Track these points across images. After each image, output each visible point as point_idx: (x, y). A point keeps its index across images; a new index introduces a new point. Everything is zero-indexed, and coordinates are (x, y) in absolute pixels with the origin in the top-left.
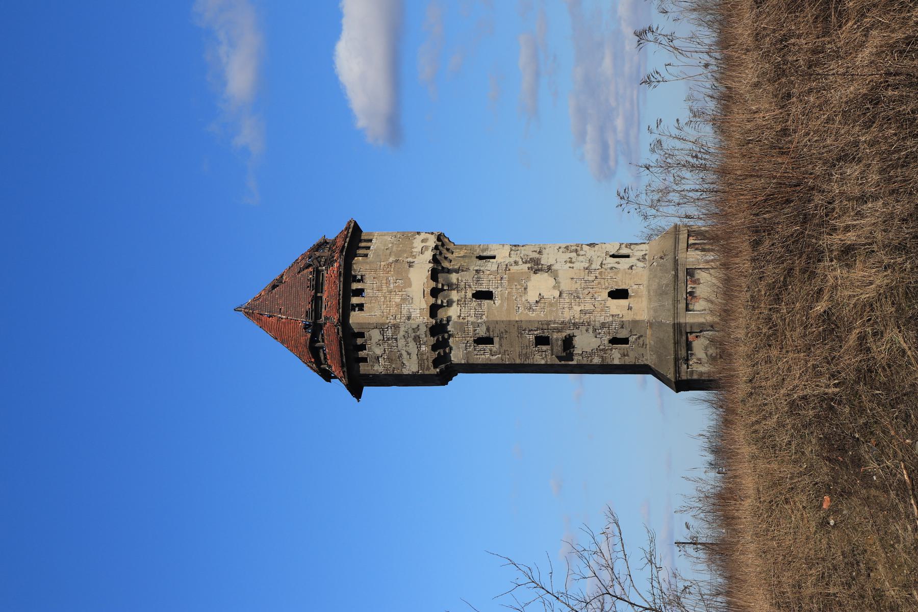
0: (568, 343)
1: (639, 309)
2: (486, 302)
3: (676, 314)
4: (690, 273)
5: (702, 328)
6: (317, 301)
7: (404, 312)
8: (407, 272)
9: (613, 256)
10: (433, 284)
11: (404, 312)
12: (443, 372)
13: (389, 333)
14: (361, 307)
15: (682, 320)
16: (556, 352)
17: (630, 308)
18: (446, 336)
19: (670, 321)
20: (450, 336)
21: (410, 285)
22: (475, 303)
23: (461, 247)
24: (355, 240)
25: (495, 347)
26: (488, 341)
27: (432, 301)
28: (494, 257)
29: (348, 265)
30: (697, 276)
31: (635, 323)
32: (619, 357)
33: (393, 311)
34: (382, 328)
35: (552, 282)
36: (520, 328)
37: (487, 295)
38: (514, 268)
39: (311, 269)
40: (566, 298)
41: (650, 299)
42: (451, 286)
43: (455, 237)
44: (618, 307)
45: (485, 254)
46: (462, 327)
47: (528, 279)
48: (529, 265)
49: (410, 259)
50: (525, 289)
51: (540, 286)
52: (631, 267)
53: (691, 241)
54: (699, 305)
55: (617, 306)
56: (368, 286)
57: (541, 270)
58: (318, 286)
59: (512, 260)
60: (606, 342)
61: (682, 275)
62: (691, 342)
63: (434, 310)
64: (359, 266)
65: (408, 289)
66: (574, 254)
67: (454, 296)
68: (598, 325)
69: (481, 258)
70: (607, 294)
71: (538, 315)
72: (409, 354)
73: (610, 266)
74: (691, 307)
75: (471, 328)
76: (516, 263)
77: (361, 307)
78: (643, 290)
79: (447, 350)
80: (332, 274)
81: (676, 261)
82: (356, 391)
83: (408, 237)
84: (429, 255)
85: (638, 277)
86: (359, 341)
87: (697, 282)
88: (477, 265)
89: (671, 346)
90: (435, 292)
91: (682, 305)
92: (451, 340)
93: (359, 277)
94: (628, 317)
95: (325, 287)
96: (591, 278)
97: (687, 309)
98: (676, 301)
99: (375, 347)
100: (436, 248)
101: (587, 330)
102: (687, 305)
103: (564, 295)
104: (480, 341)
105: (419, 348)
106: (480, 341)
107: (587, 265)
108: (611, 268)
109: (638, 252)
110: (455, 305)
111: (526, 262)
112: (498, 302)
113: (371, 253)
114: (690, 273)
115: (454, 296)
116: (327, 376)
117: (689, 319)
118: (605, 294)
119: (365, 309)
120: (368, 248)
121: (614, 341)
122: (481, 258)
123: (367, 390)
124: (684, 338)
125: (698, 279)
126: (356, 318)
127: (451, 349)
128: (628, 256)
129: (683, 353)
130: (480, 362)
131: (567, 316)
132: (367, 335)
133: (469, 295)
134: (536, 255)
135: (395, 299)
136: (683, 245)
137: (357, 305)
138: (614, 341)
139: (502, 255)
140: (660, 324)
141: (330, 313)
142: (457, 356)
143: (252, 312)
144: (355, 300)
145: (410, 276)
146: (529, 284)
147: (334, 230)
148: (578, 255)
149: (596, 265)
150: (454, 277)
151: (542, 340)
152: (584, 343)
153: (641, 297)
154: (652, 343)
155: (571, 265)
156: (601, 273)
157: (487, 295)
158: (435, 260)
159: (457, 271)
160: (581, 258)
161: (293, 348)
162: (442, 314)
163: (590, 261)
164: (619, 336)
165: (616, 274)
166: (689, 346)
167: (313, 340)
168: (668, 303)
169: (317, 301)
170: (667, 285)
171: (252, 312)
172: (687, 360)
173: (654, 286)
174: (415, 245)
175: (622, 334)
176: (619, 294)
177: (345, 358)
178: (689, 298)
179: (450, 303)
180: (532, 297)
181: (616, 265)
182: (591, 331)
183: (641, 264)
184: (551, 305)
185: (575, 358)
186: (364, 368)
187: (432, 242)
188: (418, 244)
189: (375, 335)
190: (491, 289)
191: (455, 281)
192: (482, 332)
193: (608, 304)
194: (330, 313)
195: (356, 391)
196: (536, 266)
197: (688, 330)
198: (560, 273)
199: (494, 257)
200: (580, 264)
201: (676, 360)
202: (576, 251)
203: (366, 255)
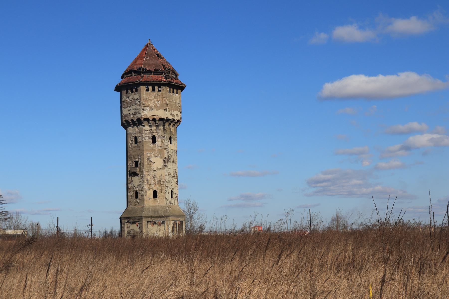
0: (135, 174)
1: (149, 202)
2: (151, 141)
3: (146, 217)
4: (163, 222)
5: (141, 228)
6: (150, 72)
7: (146, 108)
8: (162, 109)
9: (172, 191)
10: (157, 119)
11: (146, 108)
12: (126, 124)
13: (137, 102)
14: (148, 90)
15: (143, 220)
16: (134, 170)
17: (149, 199)
18: (137, 125)
19: (143, 215)
20: (138, 127)
21: (157, 110)
22: (151, 136)
23: (176, 130)
24: (180, 88)
25: (134, 145)
26: (136, 142)
27: (151, 119)
28: (171, 143)
29: (165, 84)
30: (162, 225)
31: (143, 201)
32: (134, 195)
33: (146, 103)
34: (139, 99)
35: (160, 167)
36: (141, 155)
37: (154, 141)
38: (165, 152)
39: (163, 69)
40: (153, 173)
41: (153, 206)
42: (157, 126)
43: (180, 128)
45: (172, 140)
46: (141, 131)
47: (161, 158)
48: (167, 157)
49: (168, 110)
51: (158, 162)
52: (166, 199)
53: (178, 222)
54: (150, 226)
55: (150, 193)
56: (156, 93)
57: (165, 162)
58: (157, 72)
59: (169, 151)
60: (136, 189)
61: (162, 219)
63: (147, 120)
64: (165, 89)
65: (155, 109)
66: (172, 175)
67: (154, 128)
68: (142, 186)
69: (170, 138)
71: (146, 162)
72: (130, 110)
73: (167, 190)
74: (149, 223)
75: (141, 135)
76: (168, 152)
77: (148, 90)
78: (157, 204)
79: (132, 126)
80: (162, 78)
81: (168, 216)
82: (118, 88)
83: (179, 108)
84: (170, 117)
85: (163, 201)
86: (134, 90)
87: (160, 225)
88: (167, 136)
89: (134, 216)
90: (154, 120)
91: (150, 220)
92: (136, 127)
93: (160, 89)
94: (146, 198)
95: (156, 76)
96: (161, 183)
97: (148, 222)
98: (151, 217)
99: (133, 96)
100: (174, 120)
103: (154, 172)
104: (136, 138)
105: (132, 114)
106: (136, 138)
107: (167, 181)
108: (166, 191)
109: (174, 201)
110: (150, 128)
111: (168, 156)
112: (151, 146)
113: (171, 94)
114: (163, 222)
115: (154, 128)
116: (122, 77)
117: (144, 222)
119: (147, 92)
120: (173, 92)
121: (137, 193)
122: (170, 138)
123: (119, 93)
124: (137, 221)
126: (143, 88)
127: (133, 127)
128: (172, 197)
129: (131, 220)
131: (146, 173)
134: (172, 160)
135: (152, 104)
136: (175, 219)
137: (148, 89)
138: (137, 193)
139: (172, 147)
140: (142, 211)
141: (144, 78)
142: (130, 129)
143: (149, 46)
144: (150, 88)
145: (161, 110)
146: (159, 158)
147: (182, 79)
148: (172, 177)
149: (167, 184)
150: (161, 128)
151: (136, 163)
152: (136, 181)
153: (154, 203)
155: (167, 175)
156: (164, 186)
157: (154, 141)
158: (168, 120)
159: (164, 129)
160: (171, 178)
161: (133, 64)
162: (146, 123)
163: (169, 182)
164: (138, 194)
165: (163, 193)
166: (134, 223)
167: (135, 72)
168: (151, 214)
169: (150, 72)
170: (158, 213)
171: (149, 46)
172: (128, 222)
173: (158, 208)
174: (175, 111)
175: (139, 196)
176: (155, 194)
177: (129, 85)
179: (150, 126)
180: (154, 159)
181: (167, 192)
182: (140, 183)
183: (168, 202)
184: (150, 167)
185: (130, 177)
186: (124, 92)
187: (176, 118)
188: (175, 113)
189: (136, 97)
191: (160, 128)
192: (139, 139)
194: (144, 78)
195: (118, 88)
196: (166, 161)
198: (163, 171)
199: (171, 143)
200: (167, 178)
201: (129, 218)
202: (174, 176)
203: (170, 92)
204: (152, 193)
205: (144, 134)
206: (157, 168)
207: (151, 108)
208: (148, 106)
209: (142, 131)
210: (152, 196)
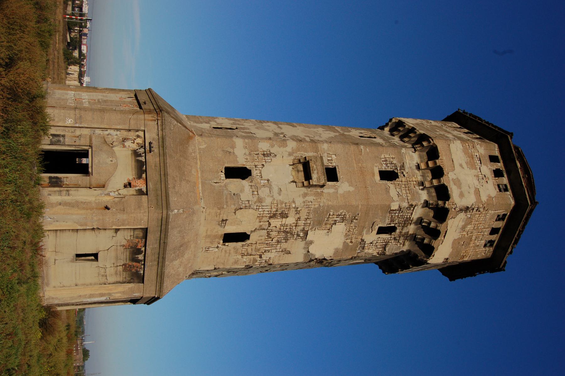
10: (434, 243)
27: (441, 227)
35: (312, 249)
60: (254, 173)
62: (140, 177)
67: (411, 229)
70: (251, 238)
74: (141, 234)
102: (145, 237)
118: (253, 238)
125: (125, 270)
127: (418, 167)
129: (152, 159)
166: (141, 168)
175: (235, 184)
178: (140, 246)
179: (420, 221)
191: (407, 243)
197: (144, 198)
206: (311, 242)
210: (231, 229)
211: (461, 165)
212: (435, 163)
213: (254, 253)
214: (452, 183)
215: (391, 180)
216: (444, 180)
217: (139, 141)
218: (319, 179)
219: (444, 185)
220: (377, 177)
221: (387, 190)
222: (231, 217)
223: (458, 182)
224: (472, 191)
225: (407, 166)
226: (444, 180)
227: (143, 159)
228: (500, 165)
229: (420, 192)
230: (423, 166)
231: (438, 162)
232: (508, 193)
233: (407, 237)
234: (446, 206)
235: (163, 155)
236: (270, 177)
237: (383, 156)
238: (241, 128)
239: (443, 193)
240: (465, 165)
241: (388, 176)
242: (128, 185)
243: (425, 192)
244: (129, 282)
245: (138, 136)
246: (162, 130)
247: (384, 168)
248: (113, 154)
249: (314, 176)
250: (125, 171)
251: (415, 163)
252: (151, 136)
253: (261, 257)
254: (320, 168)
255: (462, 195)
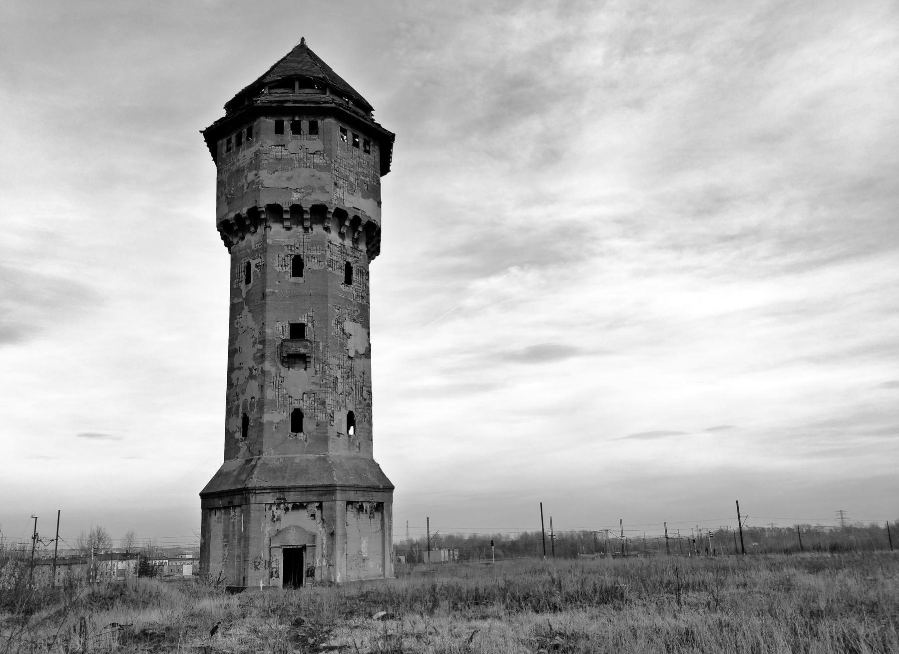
0: (301, 359)
3: (345, 488)
11: (341, 182)
15: (339, 495)
20: (306, 229)
21: (364, 197)
27: (351, 215)
35: (362, 351)
44: (340, 420)
50: (354, 320)
60: (297, 405)
62: (305, 508)
67: (348, 243)
90: (356, 220)
91: (352, 496)
92: (300, 229)
101: (314, 383)
103: (350, 362)
110: (340, 241)
118: (351, 408)
125: (373, 517)
127: (288, 229)
129: (292, 497)
130: (270, 259)
132: (314, 137)
133: (350, 260)
140: (329, 470)
154: (297, 460)
164: (305, 421)
166: (298, 506)
168: (353, 480)
175: (307, 424)
179: (342, 235)
182: (314, 388)
184: (342, 345)
190: (354, 284)
193: (343, 409)
201: (282, 490)
204: (345, 418)
205: (328, 253)
206: (357, 352)
207: (351, 185)
208: (346, 178)
209: (323, 244)
211: (289, 179)
212: (286, 212)
213: (362, 406)
214: (308, 198)
215: (303, 264)
216: (306, 206)
217: (274, 508)
218: (306, 347)
219: (310, 209)
220: (300, 280)
221: (314, 272)
222: (336, 429)
223: (310, 190)
224: (318, 174)
225: (287, 242)
226: (306, 206)
227: (290, 506)
228: (287, 124)
229: (314, 232)
230: (287, 224)
231: (286, 208)
232: (319, 122)
233: (355, 249)
234: (332, 211)
235: (289, 489)
236: (301, 391)
237: (277, 268)
238: (243, 409)
239: (319, 212)
240: (288, 174)
241: (298, 266)
242: (313, 516)
243: (314, 226)
244: (382, 513)
245: (270, 509)
246: (265, 489)
247: (289, 269)
248: (286, 530)
249: (302, 351)
250: (301, 518)
251: (283, 230)
252: (270, 498)
253: (365, 400)
254: (294, 344)
255: (323, 189)
